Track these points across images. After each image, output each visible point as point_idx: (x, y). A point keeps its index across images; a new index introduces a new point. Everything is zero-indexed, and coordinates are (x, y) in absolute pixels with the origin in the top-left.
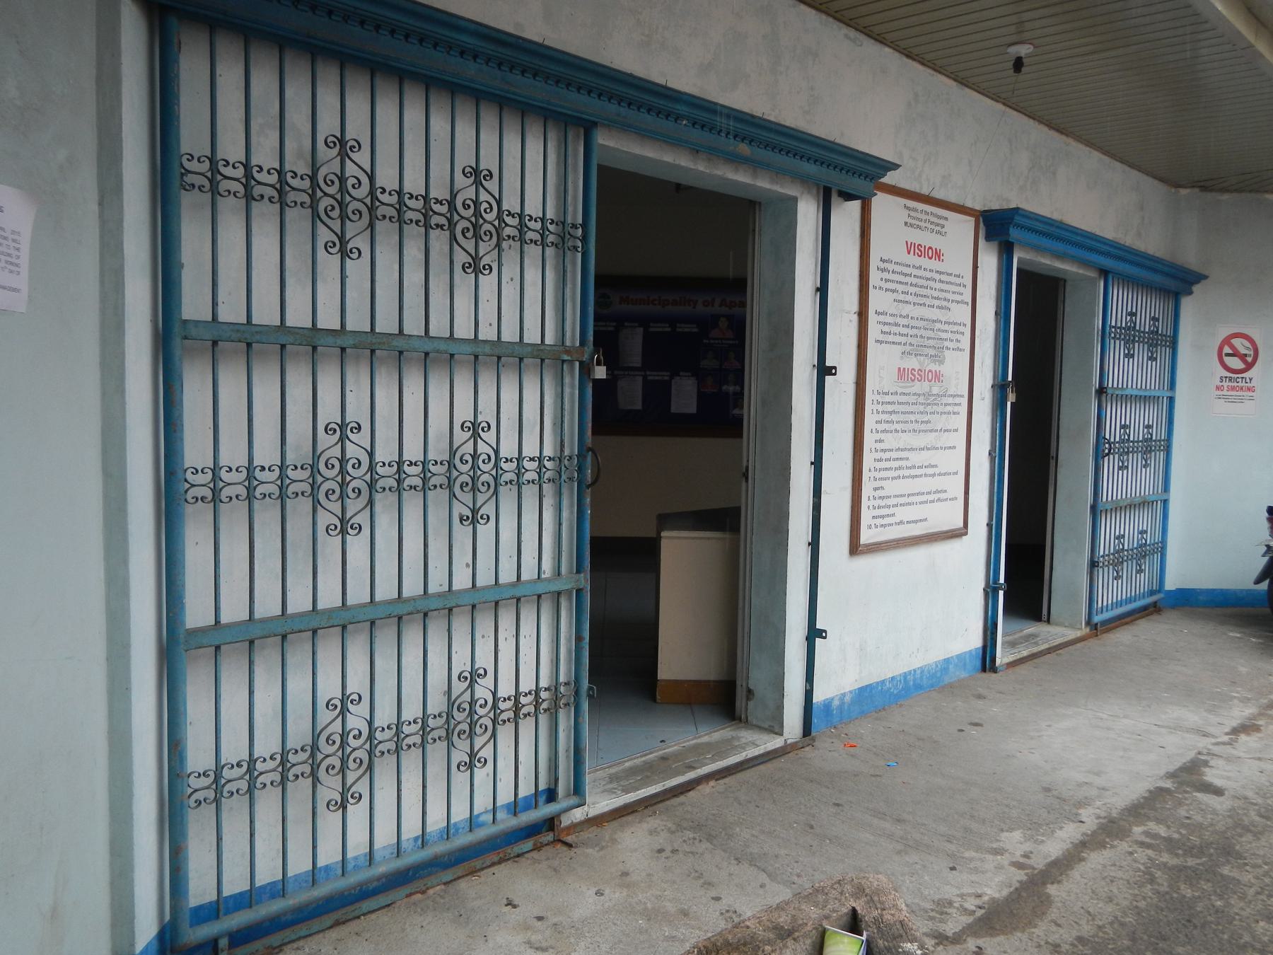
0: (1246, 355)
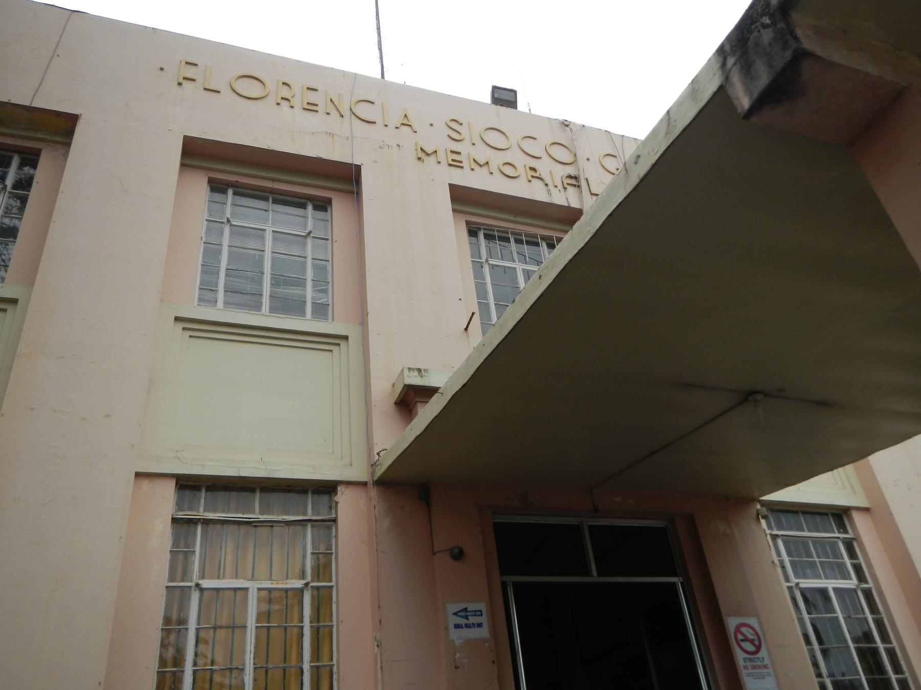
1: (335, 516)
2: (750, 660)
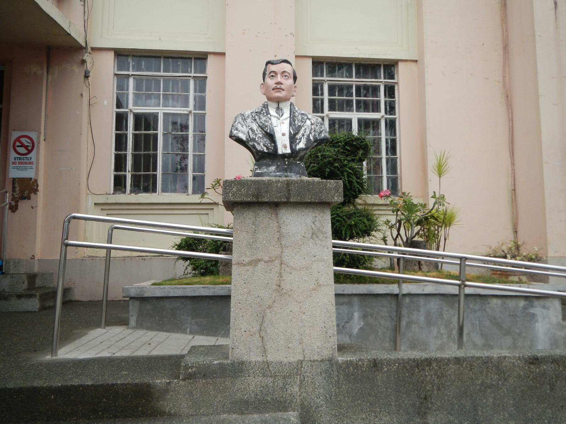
0: (28, 146)
2: (20, 158)
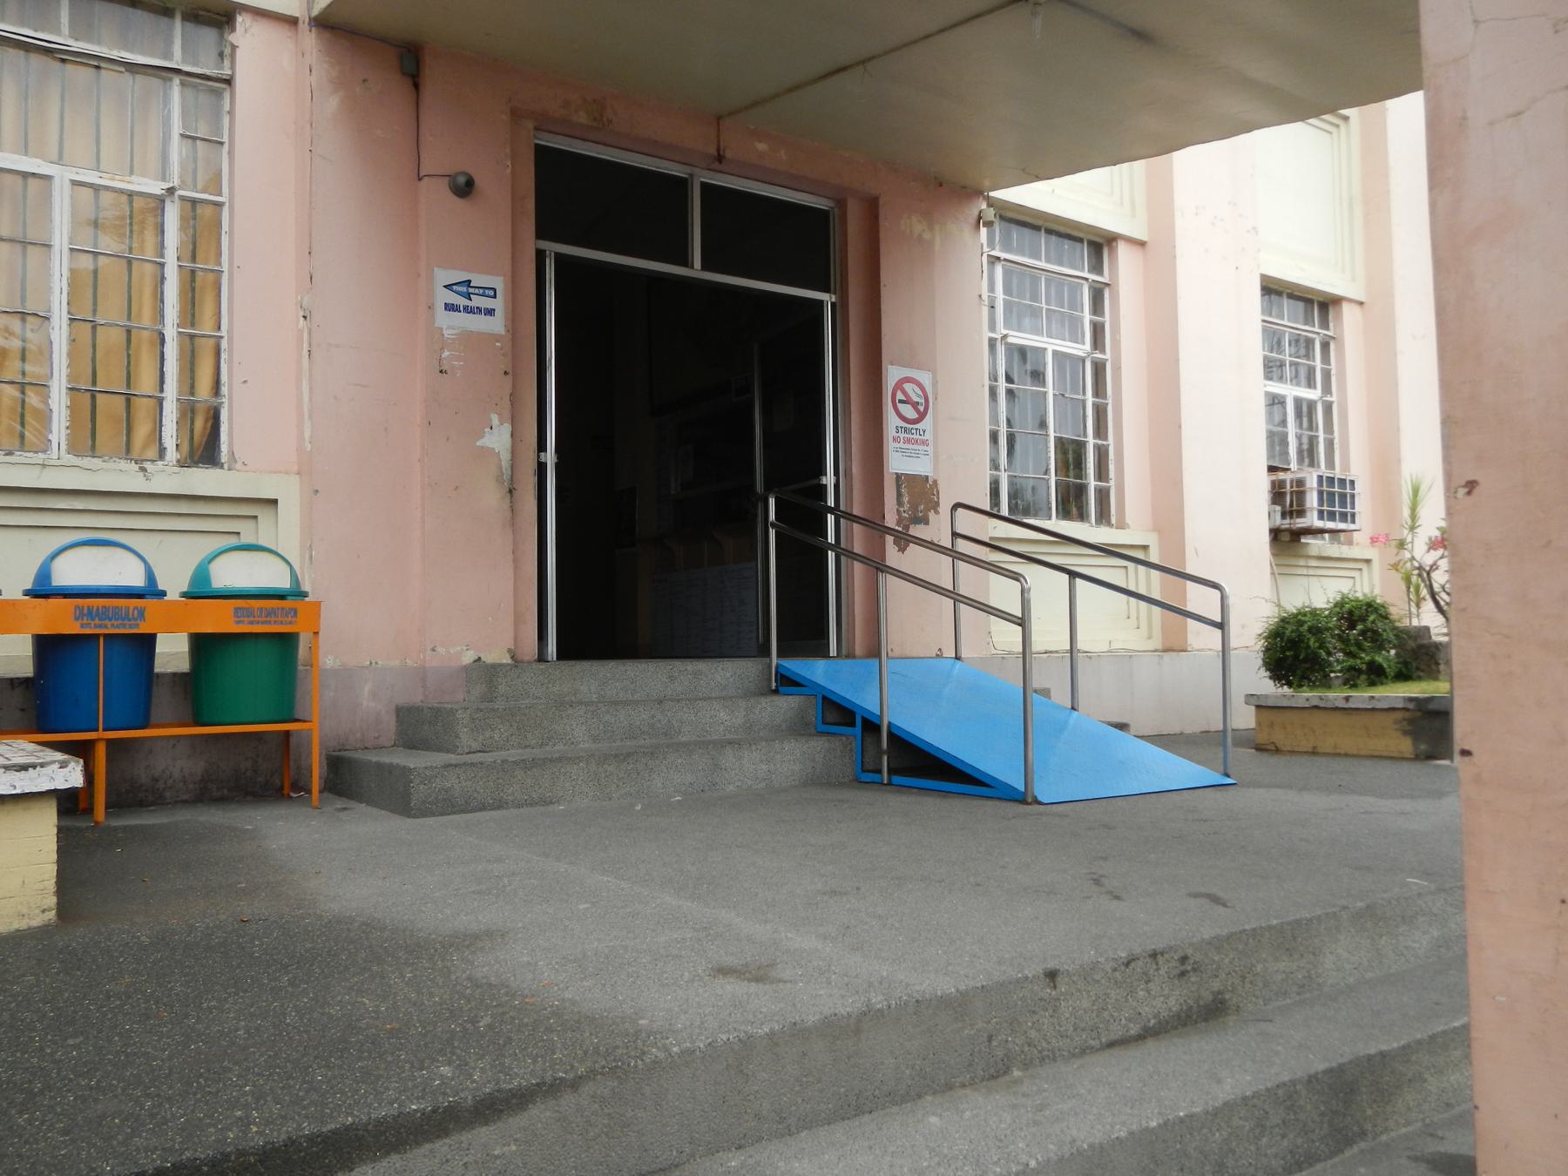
0: (918, 403)
1: (229, 72)
